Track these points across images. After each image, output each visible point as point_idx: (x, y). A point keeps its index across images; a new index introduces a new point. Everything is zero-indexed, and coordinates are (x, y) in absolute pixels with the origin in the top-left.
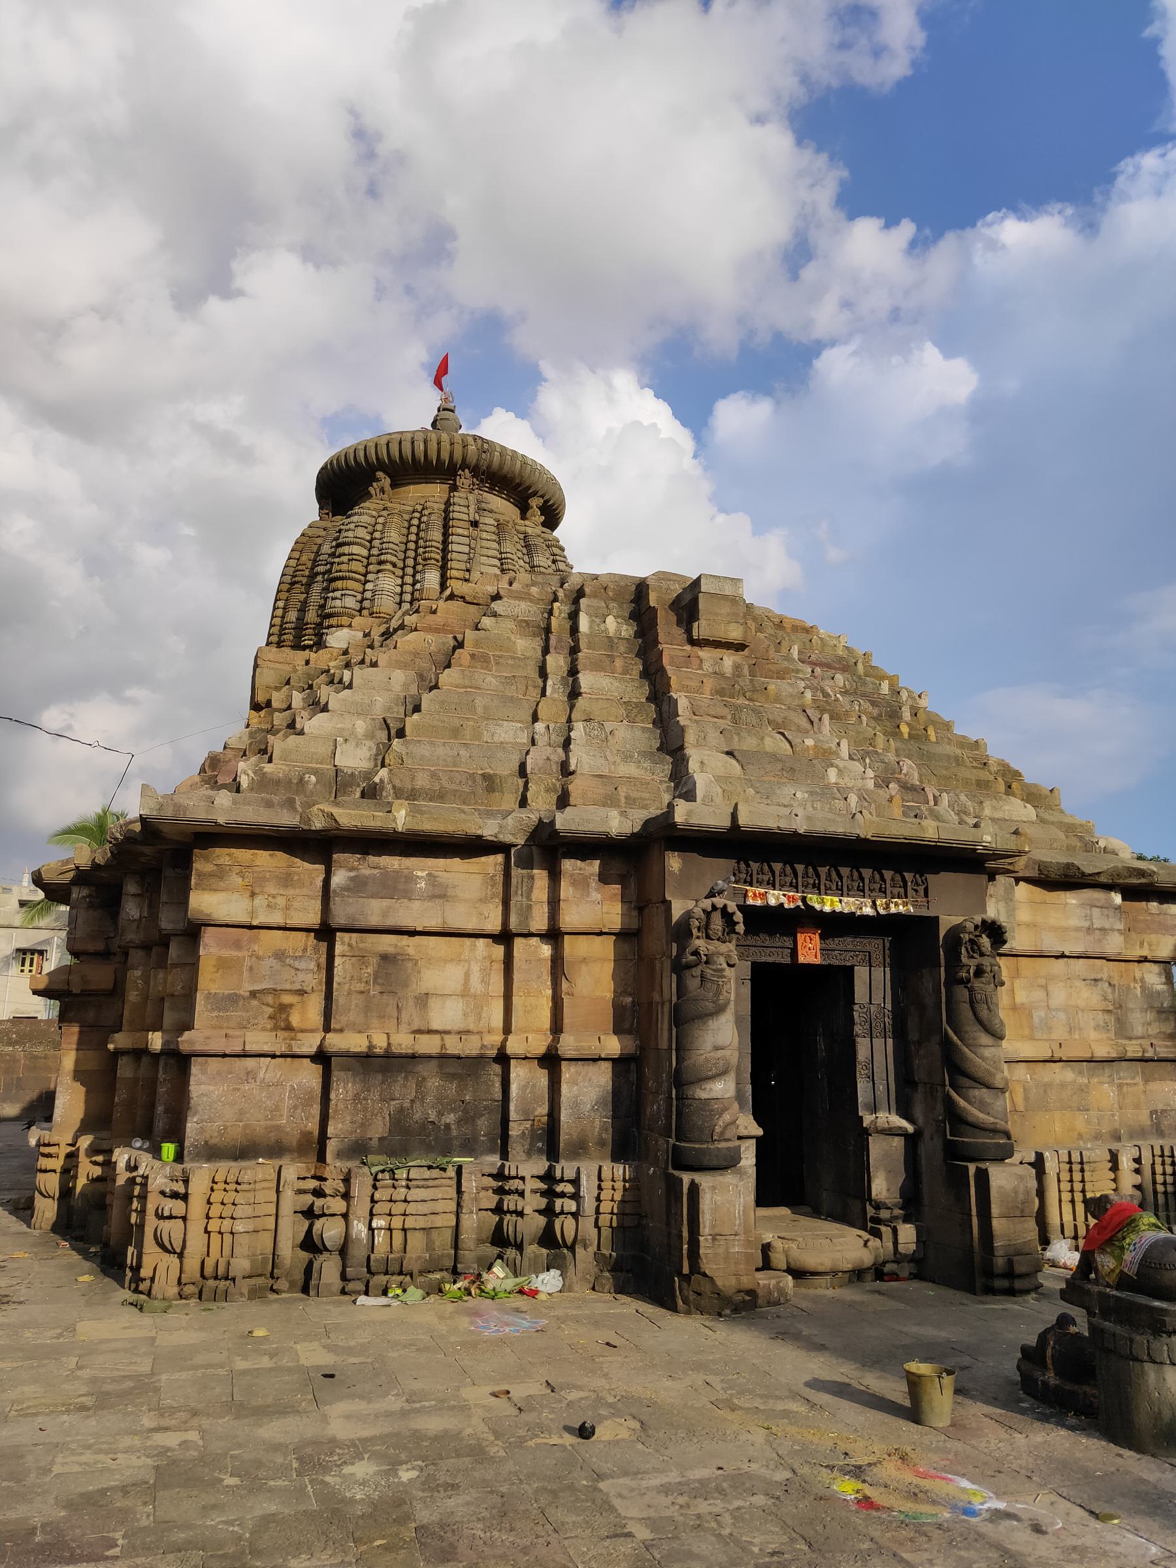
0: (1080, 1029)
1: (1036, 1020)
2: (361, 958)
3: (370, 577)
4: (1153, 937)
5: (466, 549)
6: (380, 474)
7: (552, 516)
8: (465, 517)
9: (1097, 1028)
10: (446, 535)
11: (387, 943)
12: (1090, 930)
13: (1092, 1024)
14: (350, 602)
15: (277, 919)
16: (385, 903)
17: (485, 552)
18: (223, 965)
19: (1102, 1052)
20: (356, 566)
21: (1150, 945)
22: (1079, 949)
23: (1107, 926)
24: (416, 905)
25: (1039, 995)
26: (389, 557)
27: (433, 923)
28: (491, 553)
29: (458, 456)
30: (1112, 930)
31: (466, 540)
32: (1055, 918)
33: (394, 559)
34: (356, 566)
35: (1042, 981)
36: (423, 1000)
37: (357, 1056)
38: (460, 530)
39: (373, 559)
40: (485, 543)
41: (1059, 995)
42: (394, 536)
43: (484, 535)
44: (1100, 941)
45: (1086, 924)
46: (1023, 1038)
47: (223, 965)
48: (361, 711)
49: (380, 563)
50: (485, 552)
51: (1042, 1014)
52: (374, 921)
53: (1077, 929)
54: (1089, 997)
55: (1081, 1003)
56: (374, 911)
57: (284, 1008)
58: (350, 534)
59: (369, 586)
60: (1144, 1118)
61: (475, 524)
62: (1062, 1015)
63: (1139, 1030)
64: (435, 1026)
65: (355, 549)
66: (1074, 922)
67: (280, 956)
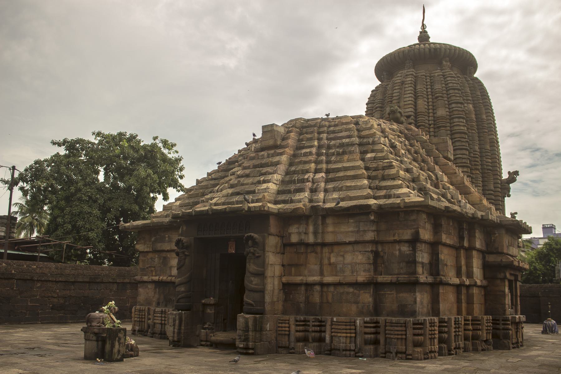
0: (357, 271)
1: (338, 269)
4: (401, 231)
5: (398, 94)
8: (399, 81)
9: (364, 271)
12: (358, 232)
13: (363, 269)
16: (161, 244)
19: (360, 279)
21: (398, 234)
22: (352, 239)
23: (366, 229)
24: (166, 244)
25: (341, 259)
27: (168, 248)
30: (369, 231)
31: (398, 90)
32: (344, 228)
35: (342, 253)
37: (157, 282)
41: (349, 258)
43: (406, 86)
44: (362, 235)
45: (356, 229)
46: (333, 275)
49: (377, 108)
51: (341, 266)
53: (352, 232)
54: (360, 258)
55: (358, 261)
60: (395, 307)
62: (349, 266)
63: (396, 271)
64: (173, 274)
66: (351, 229)
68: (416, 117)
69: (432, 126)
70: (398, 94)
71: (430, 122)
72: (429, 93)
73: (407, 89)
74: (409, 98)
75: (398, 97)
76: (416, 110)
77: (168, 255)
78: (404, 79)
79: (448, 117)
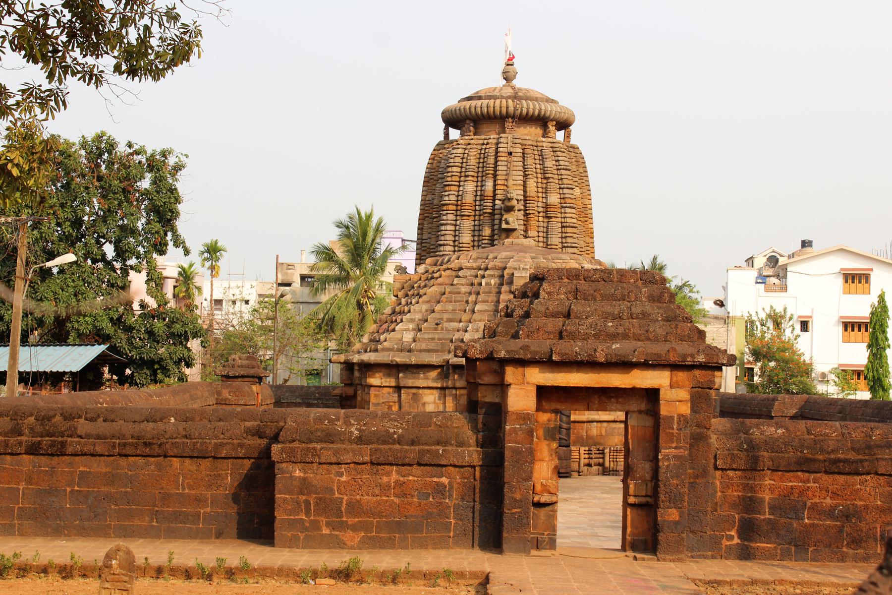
2: (408, 394)
3: (462, 183)
5: (505, 168)
6: (468, 121)
7: (564, 125)
8: (505, 150)
10: (496, 161)
11: (414, 391)
14: (453, 198)
15: (387, 384)
17: (515, 168)
18: (376, 395)
20: (454, 178)
26: (470, 173)
27: (425, 385)
28: (518, 168)
29: (504, 110)
31: (505, 163)
33: (472, 174)
34: (454, 178)
36: (424, 404)
38: (502, 158)
39: (463, 174)
40: (515, 164)
42: (473, 161)
43: (515, 159)
47: (376, 395)
48: (412, 321)
50: (515, 168)
52: (410, 385)
56: (410, 382)
57: (391, 406)
58: (452, 161)
59: (461, 188)
61: (510, 154)
65: (455, 169)
67: (389, 393)
68: (525, 201)
69: (541, 214)
70: (505, 168)
71: (540, 209)
72: (538, 171)
73: (515, 164)
74: (517, 177)
75: (505, 173)
76: (525, 191)
77: (421, 391)
78: (512, 150)
79: (559, 205)
